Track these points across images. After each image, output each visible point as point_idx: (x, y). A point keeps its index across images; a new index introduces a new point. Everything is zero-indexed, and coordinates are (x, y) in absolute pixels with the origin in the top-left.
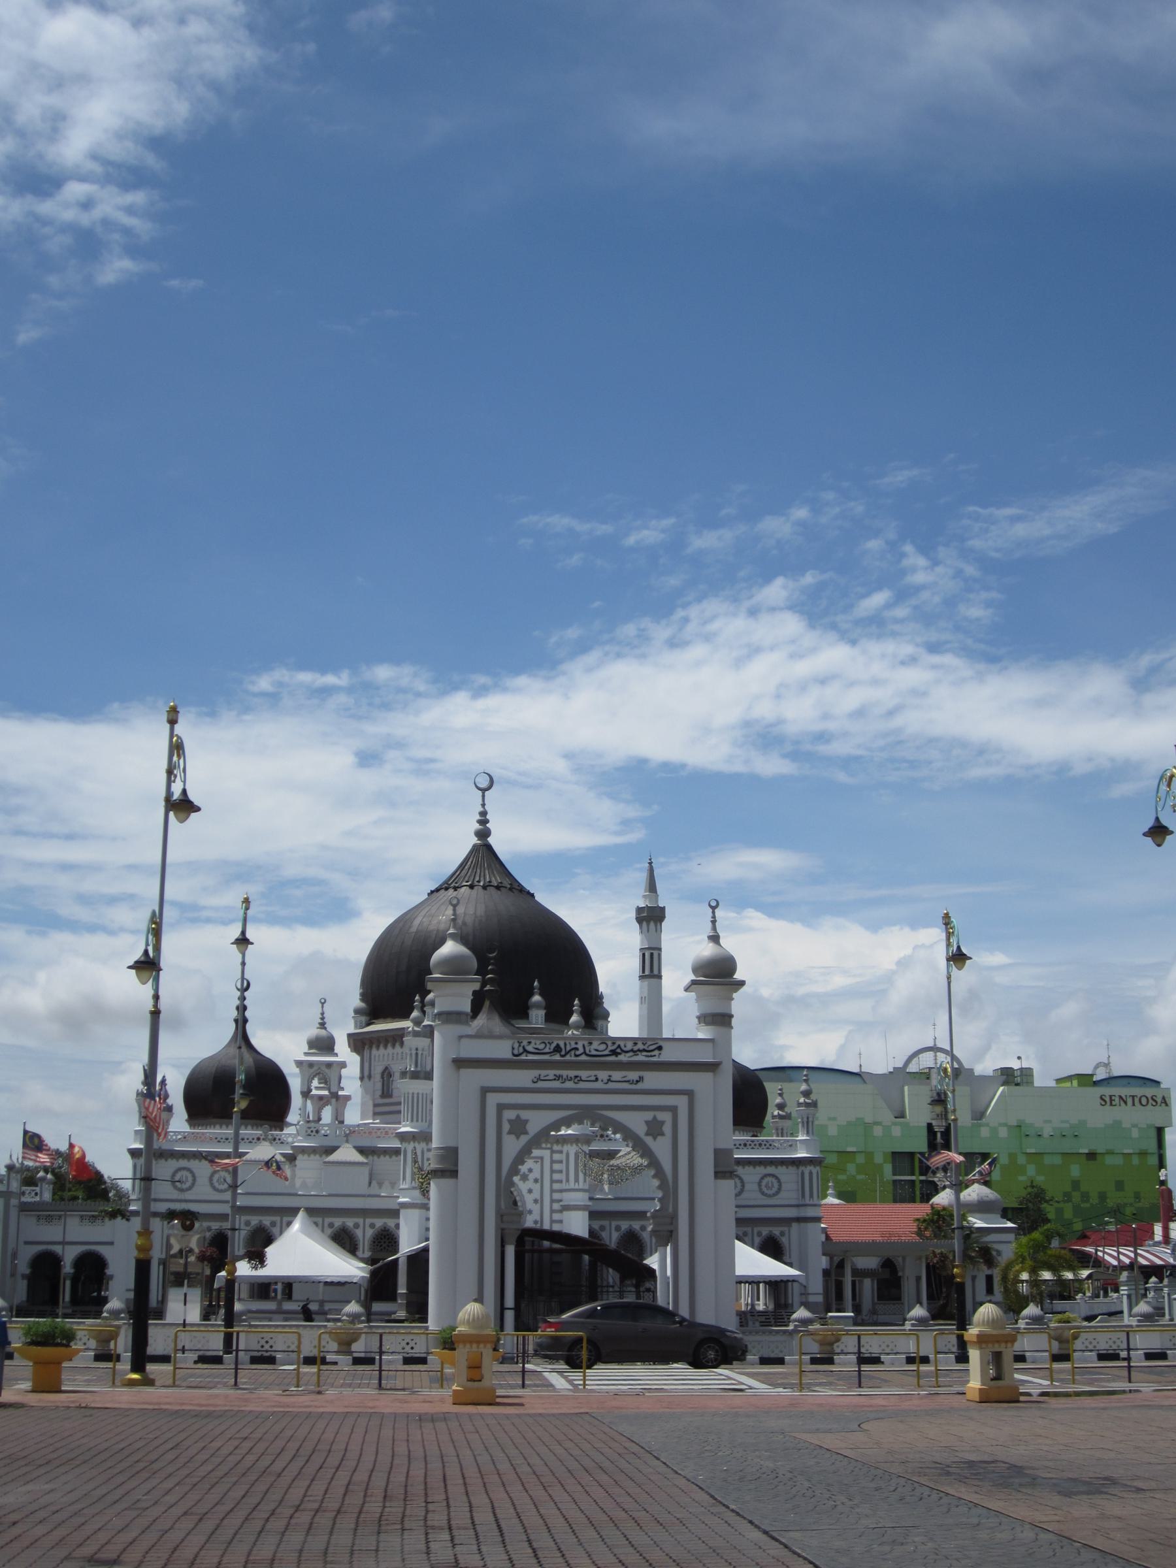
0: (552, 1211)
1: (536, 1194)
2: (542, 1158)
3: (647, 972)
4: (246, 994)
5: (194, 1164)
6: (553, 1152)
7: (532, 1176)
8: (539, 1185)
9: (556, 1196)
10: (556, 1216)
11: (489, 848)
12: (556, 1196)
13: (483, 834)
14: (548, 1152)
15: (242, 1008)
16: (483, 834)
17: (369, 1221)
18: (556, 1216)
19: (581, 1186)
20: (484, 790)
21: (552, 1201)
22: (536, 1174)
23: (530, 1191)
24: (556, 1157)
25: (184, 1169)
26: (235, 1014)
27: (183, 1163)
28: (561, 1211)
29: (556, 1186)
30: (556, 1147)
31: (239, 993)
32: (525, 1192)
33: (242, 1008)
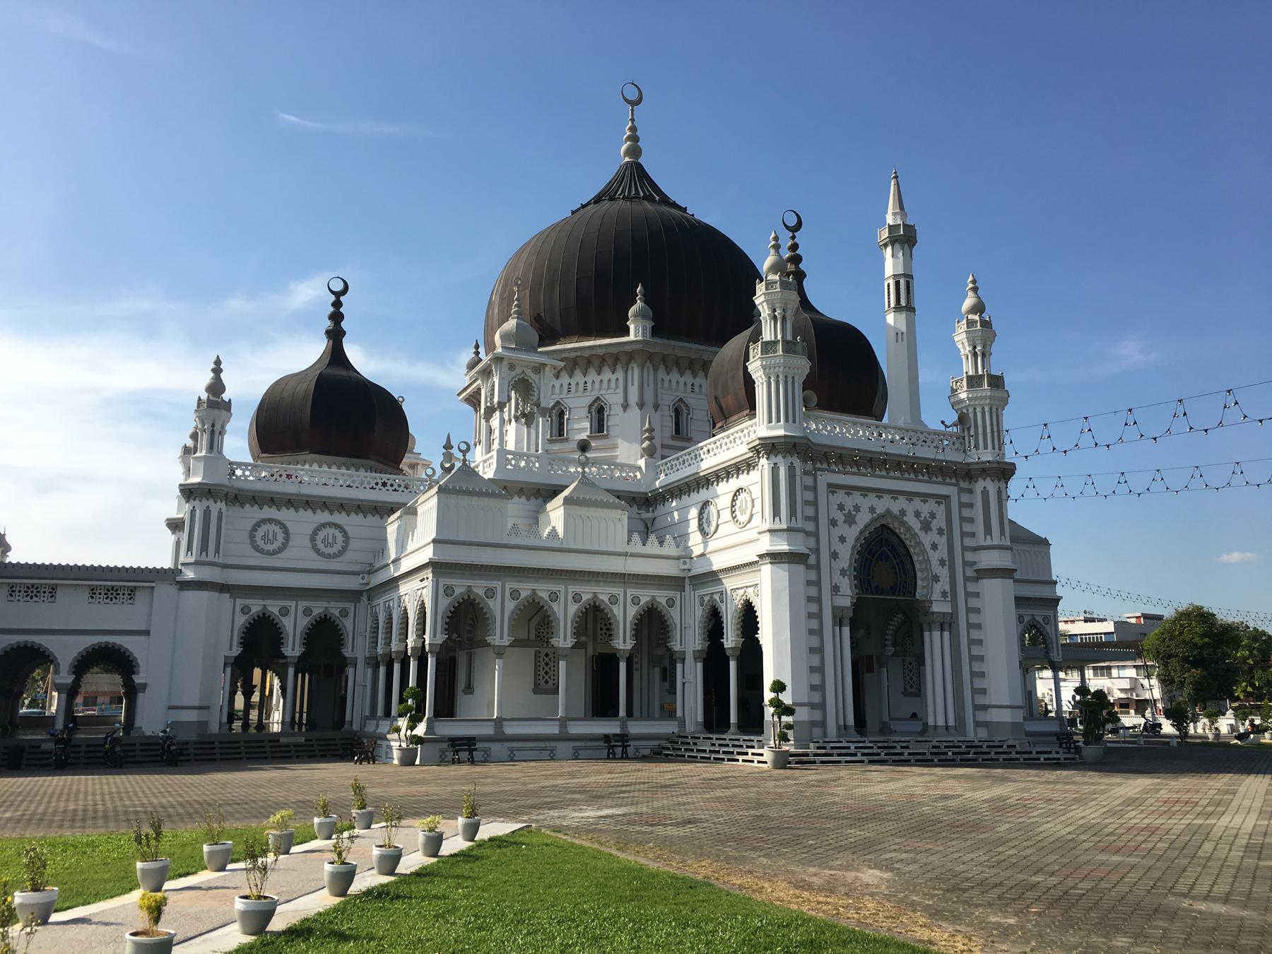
0: (966, 579)
1: (943, 552)
2: (947, 498)
3: (903, 303)
4: (342, 299)
5: (285, 515)
6: (961, 490)
7: (935, 524)
8: (945, 538)
9: (970, 557)
10: (972, 587)
11: (639, 166)
12: (970, 557)
13: (635, 151)
14: (955, 489)
15: (337, 317)
16: (635, 151)
17: (631, 592)
18: (972, 587)
19: (996, 542)
20: (634, 104)
21: (966, 564)
22: (940, 522)
23: (934, 547)
24: (965, 498)
25: (270, 521)
26: (328, 324)
27: (269, 512)
28: (977, 579)
29: (969, 542)
30: (963, 484)
31: (333, 298)
32: (928, 547)
33: (337, 317)
